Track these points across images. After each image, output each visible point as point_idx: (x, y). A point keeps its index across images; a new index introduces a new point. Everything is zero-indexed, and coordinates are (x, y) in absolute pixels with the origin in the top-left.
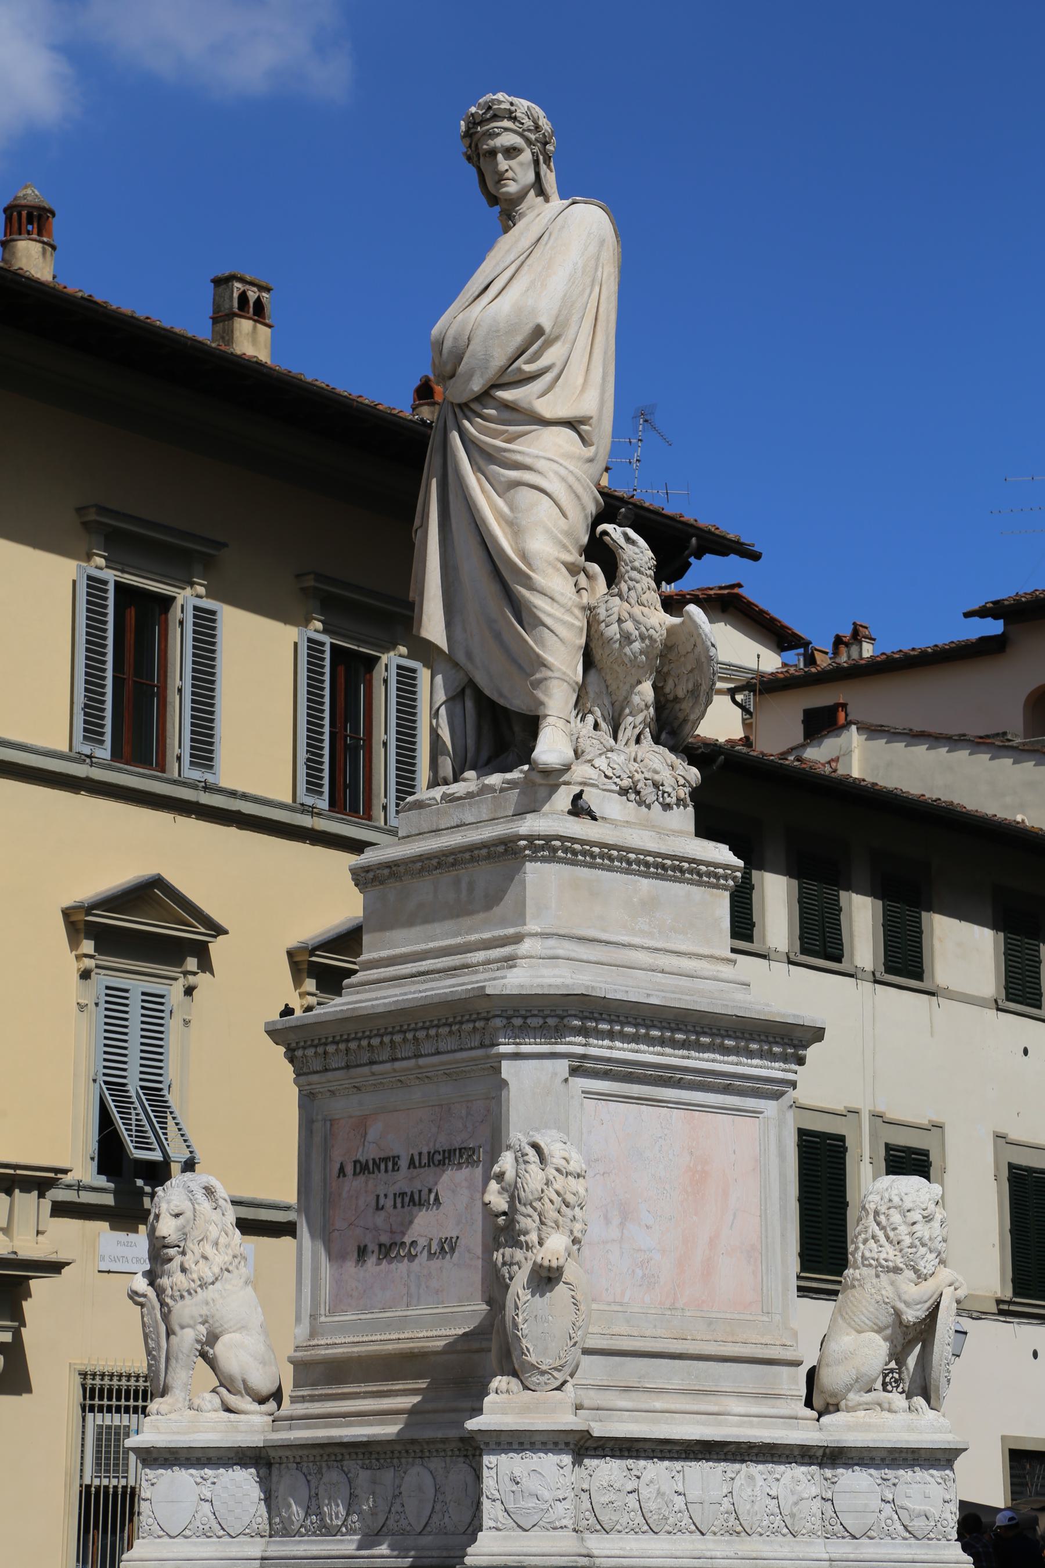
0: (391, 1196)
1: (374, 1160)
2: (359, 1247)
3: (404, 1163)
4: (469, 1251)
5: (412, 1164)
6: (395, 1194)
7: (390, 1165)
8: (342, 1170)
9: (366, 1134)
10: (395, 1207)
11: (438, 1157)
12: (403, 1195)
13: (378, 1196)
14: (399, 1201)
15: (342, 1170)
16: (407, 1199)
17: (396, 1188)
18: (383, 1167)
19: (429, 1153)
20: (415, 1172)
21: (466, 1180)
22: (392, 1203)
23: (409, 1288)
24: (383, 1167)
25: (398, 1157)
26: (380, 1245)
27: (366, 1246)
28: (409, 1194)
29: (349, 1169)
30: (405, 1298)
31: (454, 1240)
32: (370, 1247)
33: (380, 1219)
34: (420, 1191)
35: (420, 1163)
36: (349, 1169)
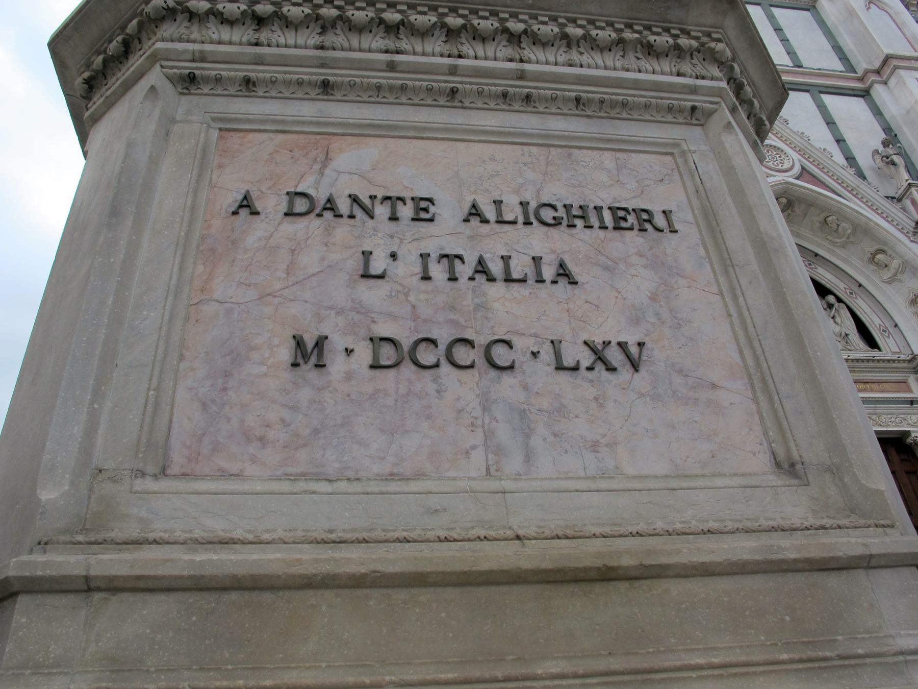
0: (415, 258)
1: (355, 199)
2: (299, 342)
3: (448, 212)
4: (680, 371)
5: (475, 212)
6: (424, 257)
7: (406, 211)
8: (246, 204)
9: (327, 158)
10: (426, 278)
11: (547, 215)
12: (451, 259)
13: (367, 255)
14: (438, 271)
15: (246, 204)
16: (464, 270)
17: (432, 247)
18: (382, 211)
19: (524, 205)
20: (485, 229)
21: (640, 254)
22: (418, 269)
23: (489, 434)
24: (382, 211)
25: (430, 200)
26: (378, 341)
27: (320, 343)
28: (471, 261)
29: (272, 204)
30: (478, 458)
31: (634, 350)
32: (338, 342)
33: (372, 295)
34: (506, 259)
35: (499, 213)
36: (272, 204)
